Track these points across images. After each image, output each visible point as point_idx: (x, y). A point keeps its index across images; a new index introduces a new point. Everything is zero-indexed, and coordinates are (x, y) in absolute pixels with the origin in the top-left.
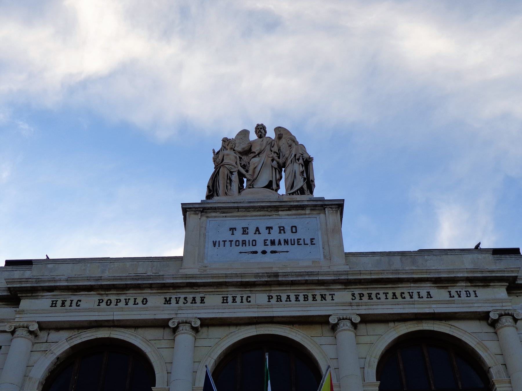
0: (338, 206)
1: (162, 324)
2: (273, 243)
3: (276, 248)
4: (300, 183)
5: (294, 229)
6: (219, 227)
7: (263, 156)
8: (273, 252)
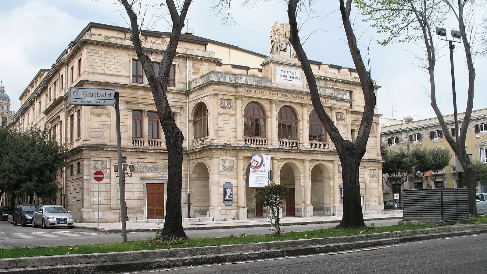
8: (291, 81)
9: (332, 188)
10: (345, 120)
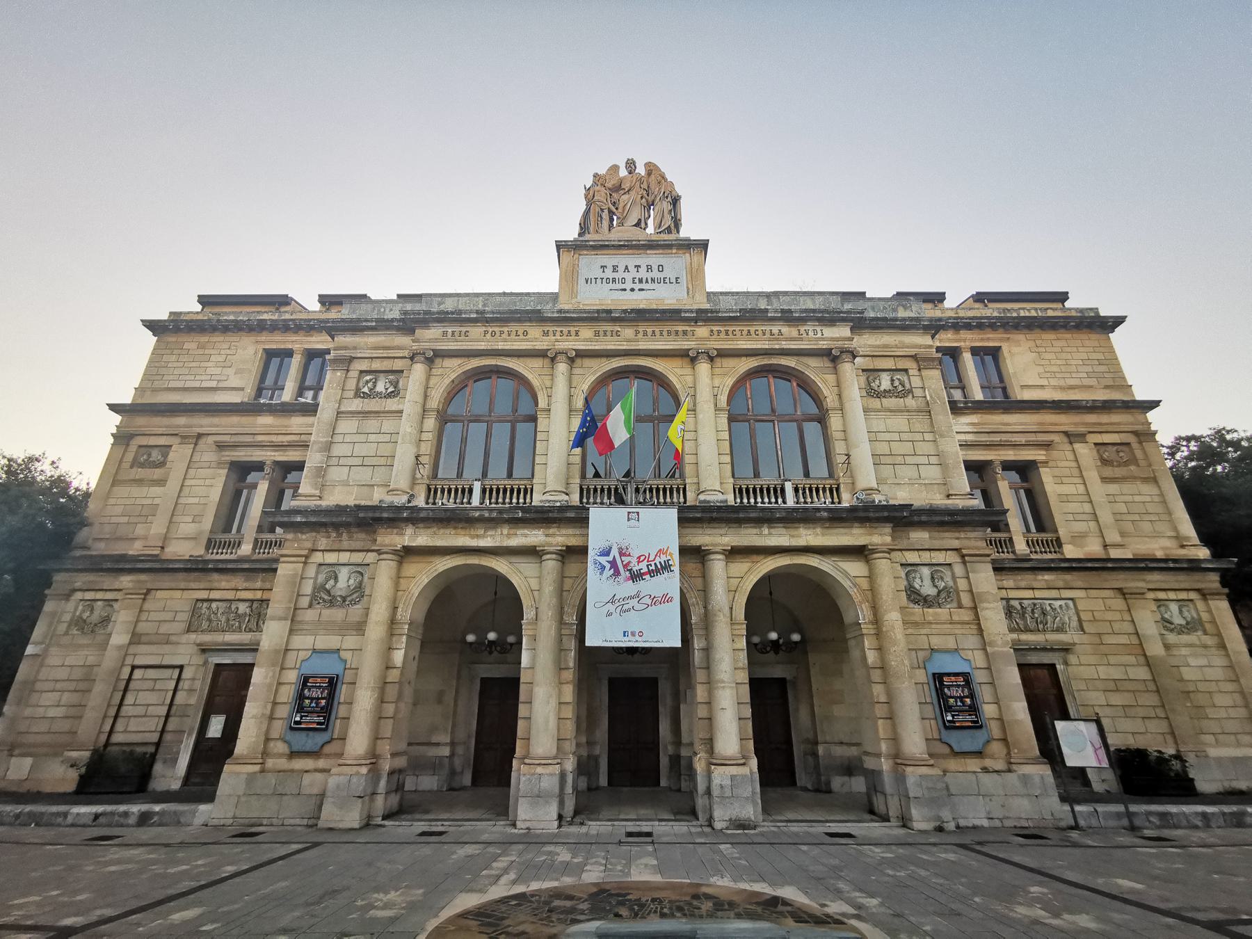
0: (703, 246)
1: (542, 354)
2: (641, 281)
3: (644, 286)
4: (668, 222)
5: (661, 268)
6: (590, 265)
7: (633, 193)
9: (876, 675)
10: (918, 392)
